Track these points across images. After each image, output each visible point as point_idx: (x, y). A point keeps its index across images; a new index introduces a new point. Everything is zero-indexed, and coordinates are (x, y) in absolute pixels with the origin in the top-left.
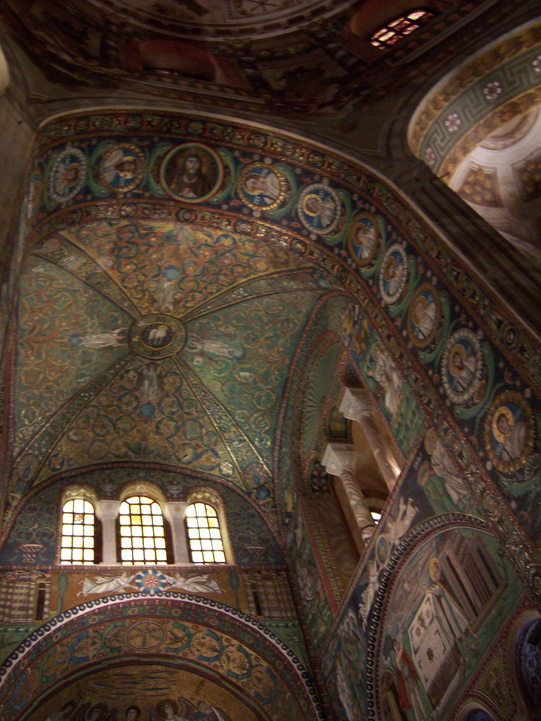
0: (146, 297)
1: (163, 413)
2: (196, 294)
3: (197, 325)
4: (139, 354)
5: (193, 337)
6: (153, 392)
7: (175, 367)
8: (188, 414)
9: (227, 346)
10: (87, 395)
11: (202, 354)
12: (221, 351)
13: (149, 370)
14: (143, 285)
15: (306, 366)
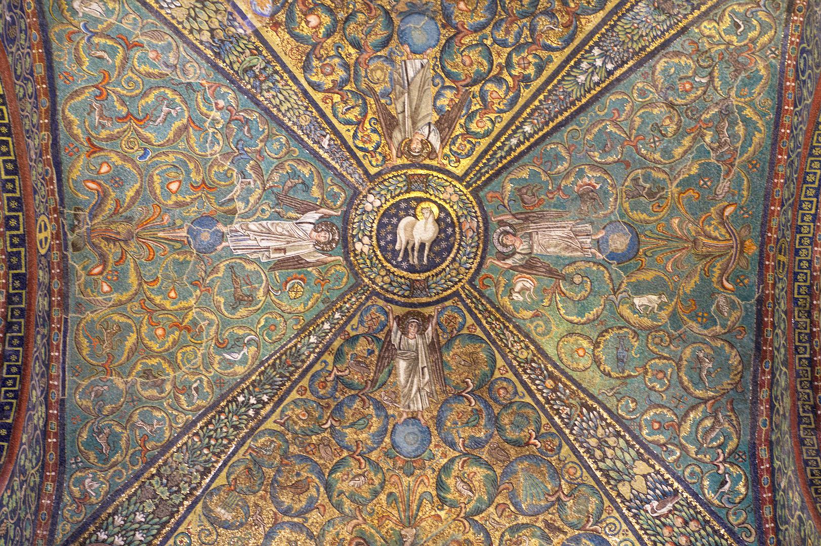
0: (370, 116)
1: (453, 445)
2: (490, 87)
3: (509, 187)
4: (378, 295)
5: (501, 223)
6: (419, 390)
7: (470, 320)
8: (516, 443)
9: (589, 227)
10: (253, 400)
11: (530, 265)
12: (576, 244)
13: (405, 333)
14: (356, 80)
15: (799, 230)
